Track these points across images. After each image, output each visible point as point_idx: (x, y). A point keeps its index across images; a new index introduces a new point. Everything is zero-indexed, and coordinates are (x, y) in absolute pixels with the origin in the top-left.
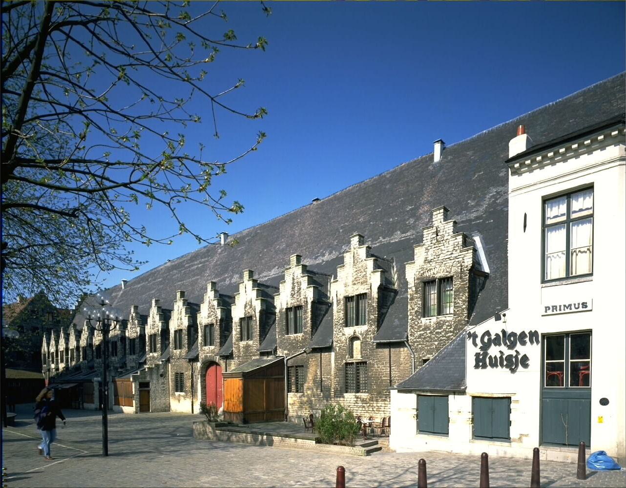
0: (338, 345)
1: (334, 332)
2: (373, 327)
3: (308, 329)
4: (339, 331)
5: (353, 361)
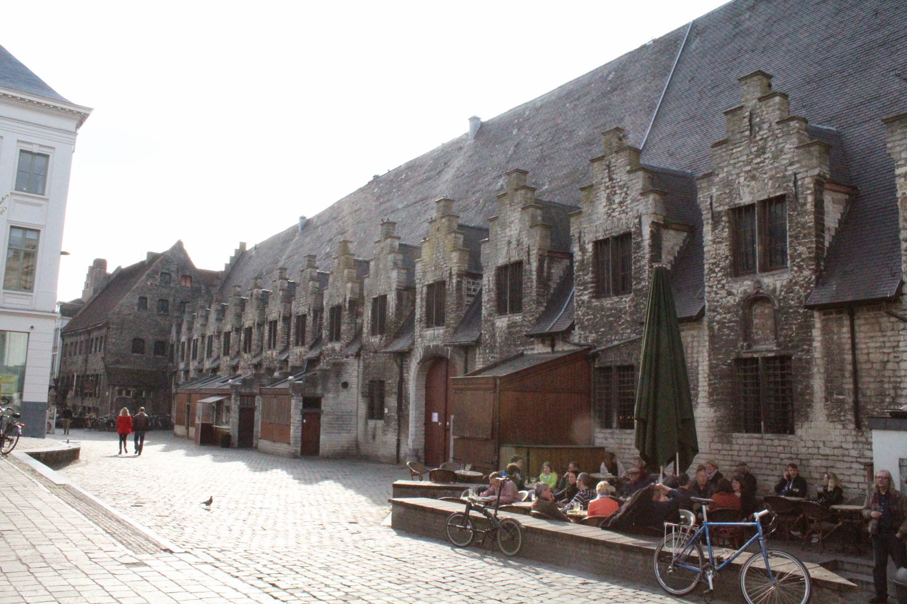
0: (718, 317)
1: (707, 289)
2: (806, 273)
3: (643, 283)
4: (719, 286)
5: (755, 356)
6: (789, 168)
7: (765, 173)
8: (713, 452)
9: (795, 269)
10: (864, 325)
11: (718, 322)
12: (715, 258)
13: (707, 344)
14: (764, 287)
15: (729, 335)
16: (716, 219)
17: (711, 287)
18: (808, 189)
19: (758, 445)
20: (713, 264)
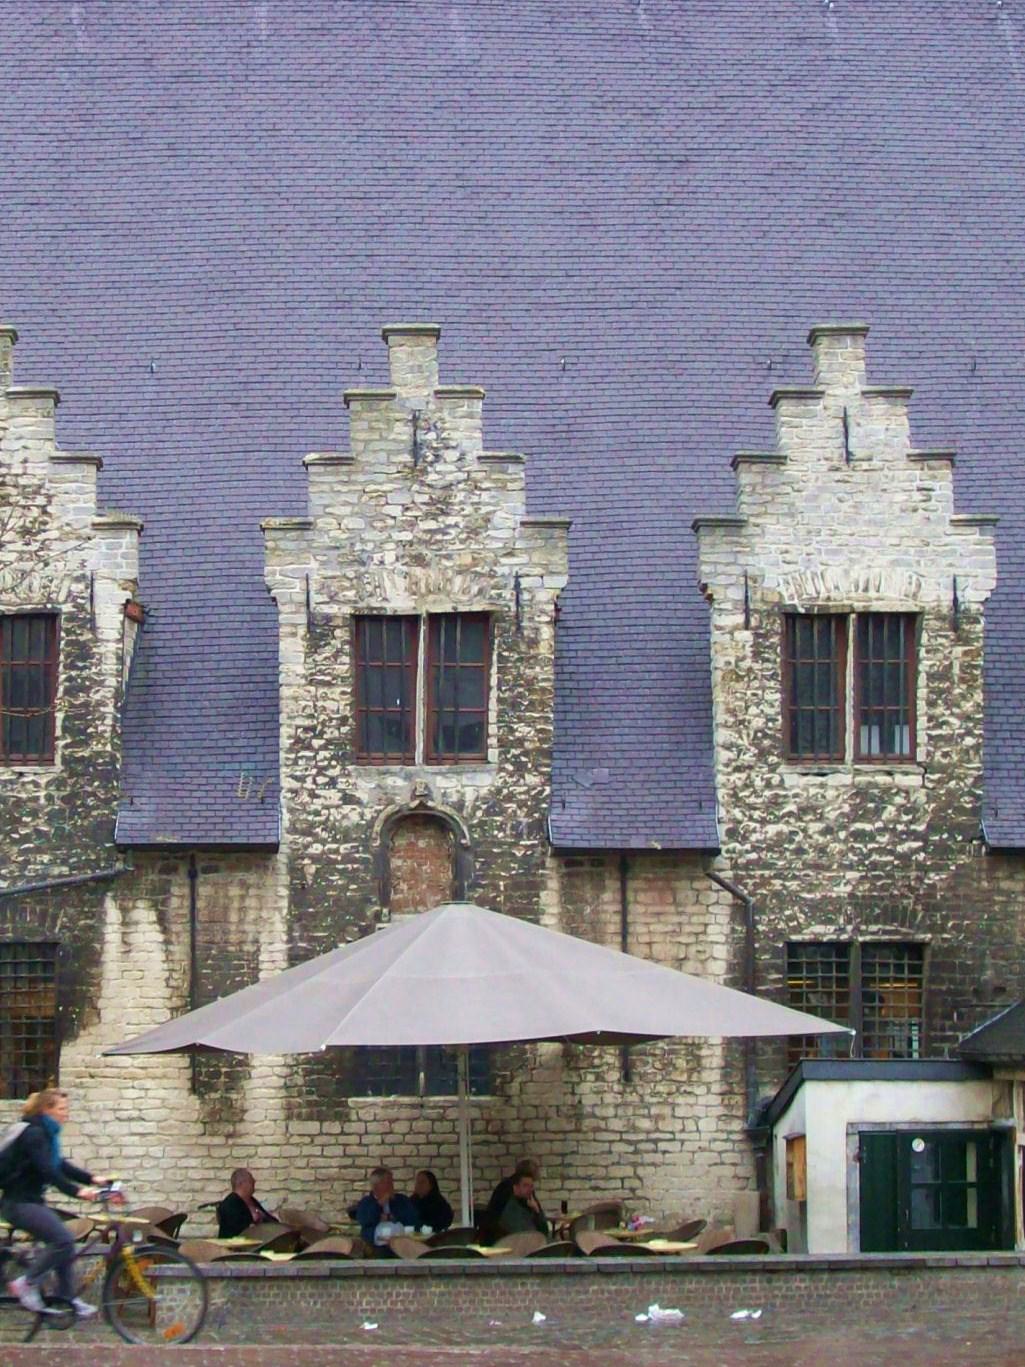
0: (316, 849)
2: (531, 779)
6: (504, 560)
7: (448, 557)
8: (295, 1140)
9: (510, 768)
10: (644, 891)
11: (315, 859)
12: (311, 716)
13: (284, 903)
14: (436, 795)
15: (345, 888)
16: (318, 631)
17: (301, 779)
18: (543, 612)
19: (412, 1120)
20: (306, 729)
